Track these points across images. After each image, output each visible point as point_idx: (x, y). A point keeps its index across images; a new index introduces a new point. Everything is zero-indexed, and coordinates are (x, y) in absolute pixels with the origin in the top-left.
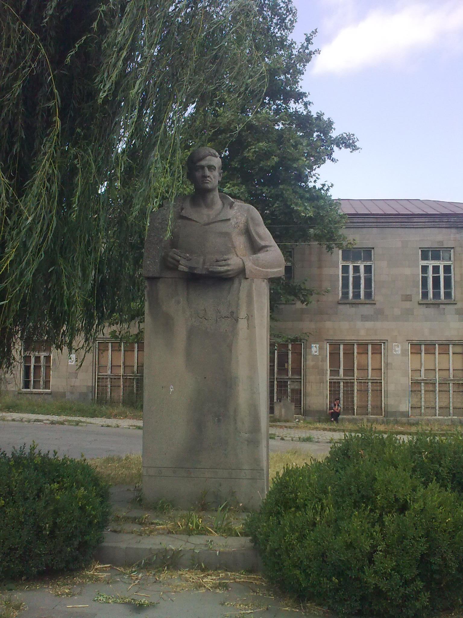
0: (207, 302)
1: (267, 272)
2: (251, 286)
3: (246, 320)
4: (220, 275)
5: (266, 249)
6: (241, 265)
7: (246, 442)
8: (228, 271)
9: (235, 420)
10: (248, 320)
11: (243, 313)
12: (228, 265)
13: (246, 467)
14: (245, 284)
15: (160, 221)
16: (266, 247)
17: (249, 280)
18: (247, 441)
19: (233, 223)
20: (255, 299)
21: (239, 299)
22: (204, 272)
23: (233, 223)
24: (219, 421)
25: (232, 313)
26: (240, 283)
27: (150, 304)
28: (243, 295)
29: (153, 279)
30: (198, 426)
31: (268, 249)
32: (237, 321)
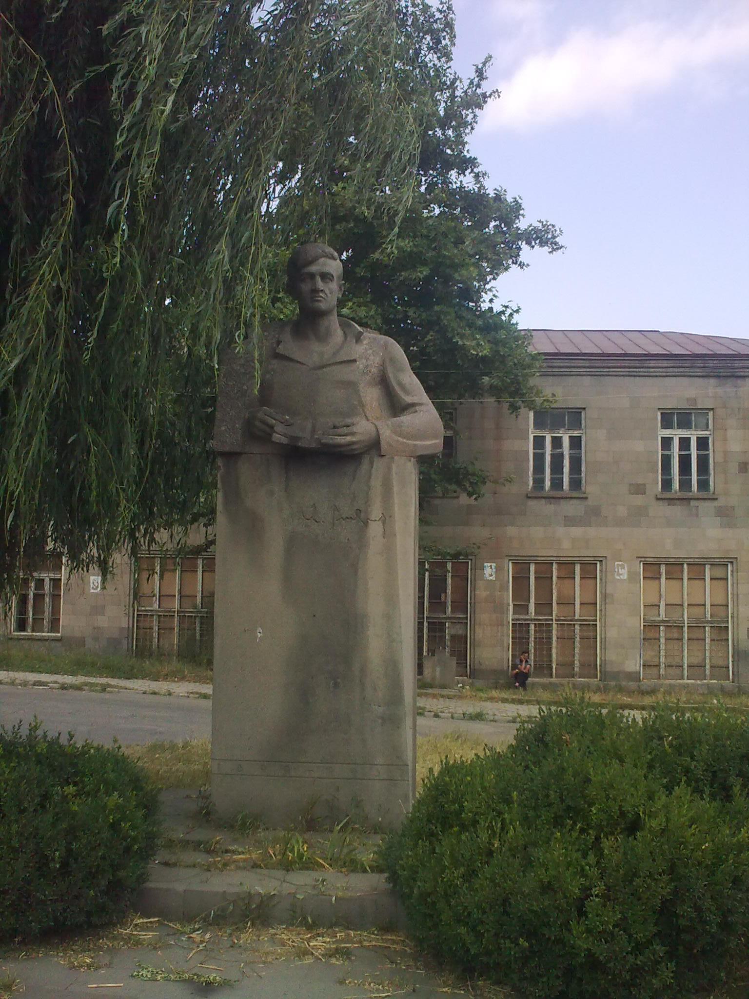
0: (317, 492)
1: (415, 445)
2: (389, 469)
4: (342, 449)
5: (413, 409)
6: (374, 433)
7: (380, 721)
8: (353, 443)
10: (384, 523)
11: (376, 512)
12: (353, 434)
13: (380, 760)
14: (379, 465)
15: (242, 361)
16: (413, 405)
17: (385, 459)
18: (382, 718)
21: (369, 487)
22: (314, 445)
24: (336, 685)
26: (372, 464)
27: (226, 497)
28: (376, 483)
29: (231, 456)
32: (366, 524)
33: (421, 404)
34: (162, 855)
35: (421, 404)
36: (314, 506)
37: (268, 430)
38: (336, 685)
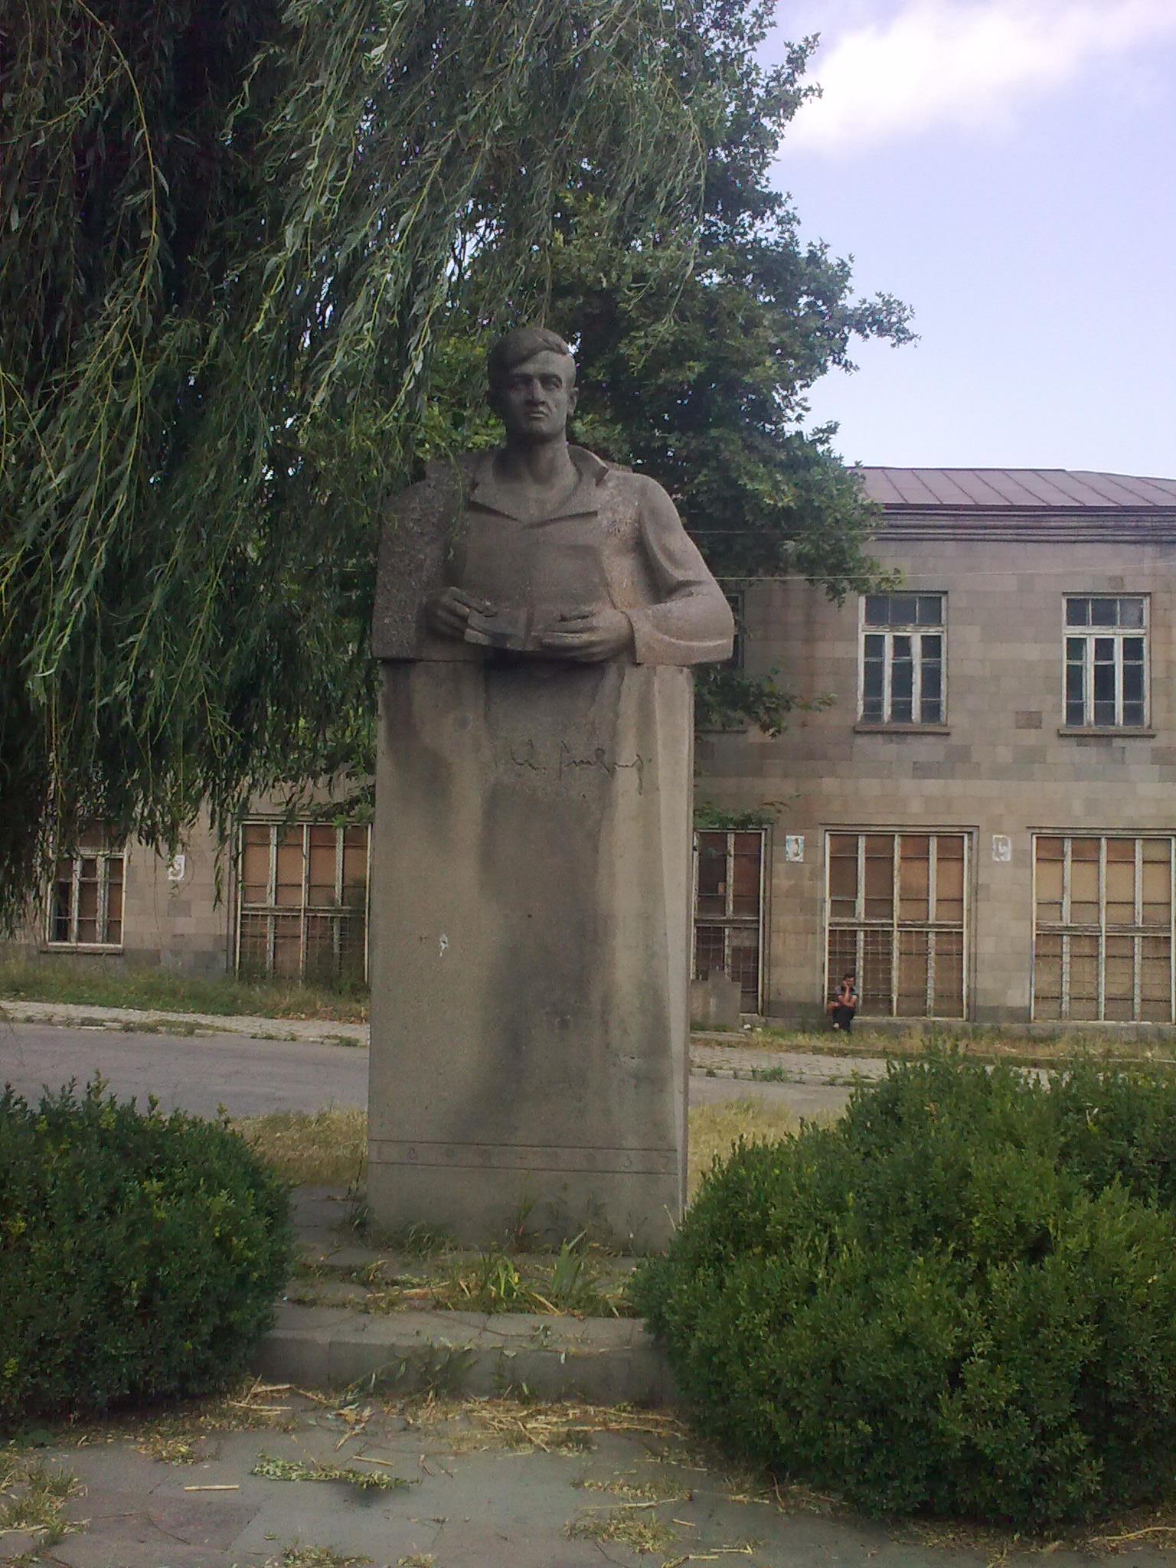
0: (536, 721)
1: (689, 648)
2: (649, 683)
3: (634, 769)
7: (633, 1081)
8: (592, 644)
9: (605, 1023)
10: (640, 770)
11: (627, 753)
12: (591, 629)
13: (631, 1142)
14: (633, 678)
15: (416, 516)
17: (643, 670)
19: (605, 522)
20: (659, 715)
21: (617, 715)
22: (530, 648)
23: (605, 522)
24: (564, 1024)
25: (600, 752)
26: (621, 677)
27: (391, 727)
28: (629, 706)
29: (398, 665)
30: (512, 1040)
31: (693, 589)
32: (612, 771)
33: (699, 583)
34: (294, 1287)
35: (699, 583)
36: (531, 743)
37: (457, 623)
38: (564, 1024)
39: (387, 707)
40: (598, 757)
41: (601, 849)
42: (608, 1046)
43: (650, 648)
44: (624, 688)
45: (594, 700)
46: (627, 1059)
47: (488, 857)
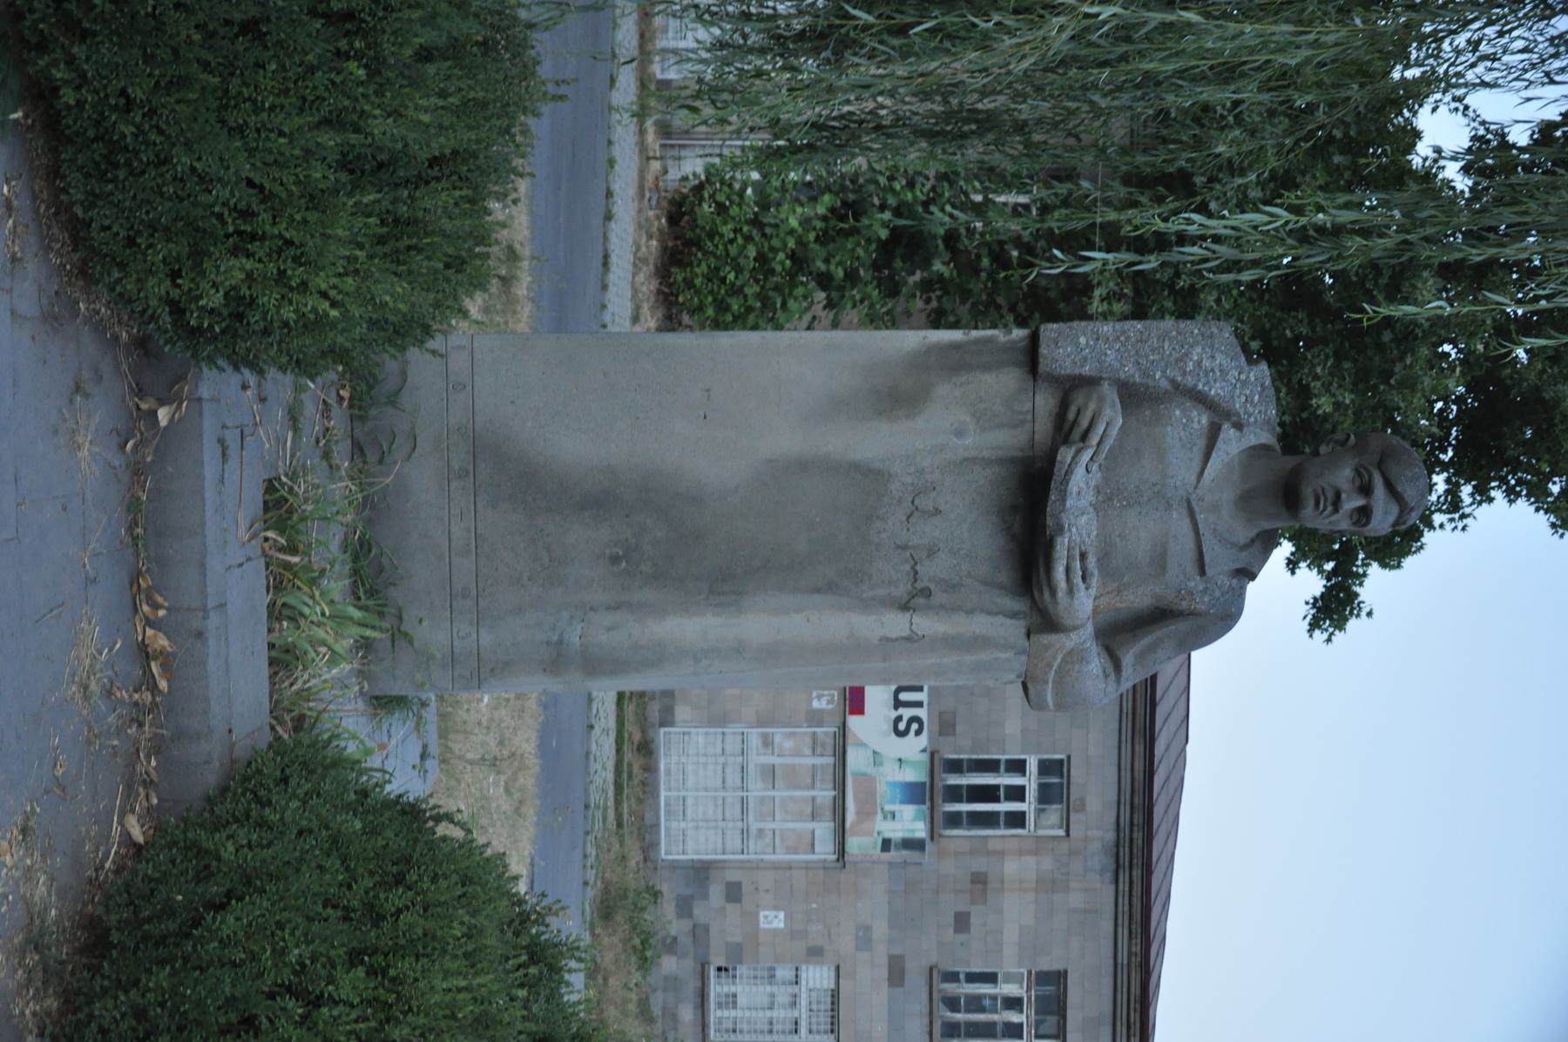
0: (967, 534)
1: (1046, 682)
2: (1006, 647)
3: (906, 633)
4: (1042, 570)
5: (1110, 670)
6: (1067, 621)
7: (555, 638)
8: (1053, 592)
9: (617, 607)
10: (908, 639)
11: (926, 624)
12: (1071, 591)
13: (486, 638)
14: (1013, 630)
15: (1206, 363)
16: (1117, 666)
17: (1022, 642)
18: (560, 642)
19: (1192, 584)
20: (969, 658)
21: (970, 612)
22: (1050, 522)
23: (1192, 584)
24: (615, 560)
25: (926, 593)
26: (1014, 615)
27: (956, 346)
28: (980, 625)
29: (1031, 357)
30: (598, 500)
31: (1113, 676)
32: (905, 607)
33: (1118, 681)
34: (249, 376)
35: (1118, 681)
36: (937, 512)
37: (1077, 434)
38: (615, 560)
39: (977, 341)
40: (922, 590)
41: (816, 597)
42: (592, 609)
43: (1047, 648)
44: (1001, 619)
45: (986, 584)
46: (579, 632)
47: (804, 466)
